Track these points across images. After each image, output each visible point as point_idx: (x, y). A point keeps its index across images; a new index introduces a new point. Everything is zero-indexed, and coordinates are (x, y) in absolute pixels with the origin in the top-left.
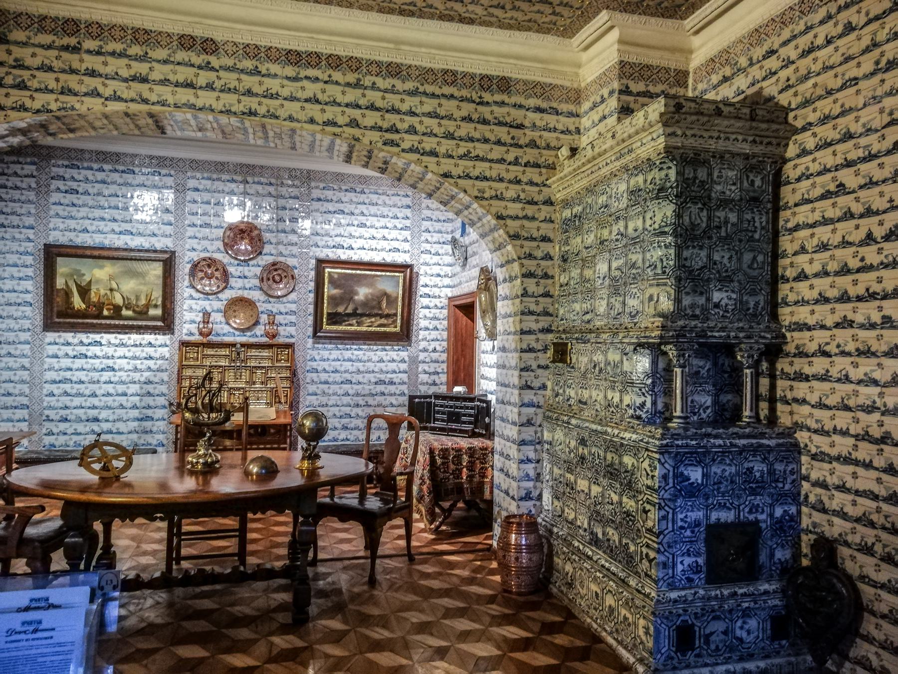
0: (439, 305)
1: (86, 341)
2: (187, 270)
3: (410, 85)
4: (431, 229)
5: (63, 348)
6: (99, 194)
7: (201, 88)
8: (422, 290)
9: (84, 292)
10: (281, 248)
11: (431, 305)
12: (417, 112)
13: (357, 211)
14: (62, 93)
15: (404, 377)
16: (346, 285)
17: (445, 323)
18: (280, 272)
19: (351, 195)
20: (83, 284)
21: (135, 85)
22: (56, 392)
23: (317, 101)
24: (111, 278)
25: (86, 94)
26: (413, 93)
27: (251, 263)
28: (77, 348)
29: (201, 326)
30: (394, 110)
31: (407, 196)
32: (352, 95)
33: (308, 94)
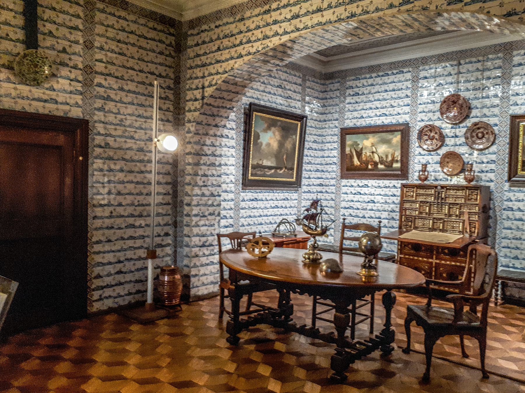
6: (369, 93)
7: (325, 9)
9: (359, 154)
10: (485, 111)
20: (359, 150)
24: (373, 145)
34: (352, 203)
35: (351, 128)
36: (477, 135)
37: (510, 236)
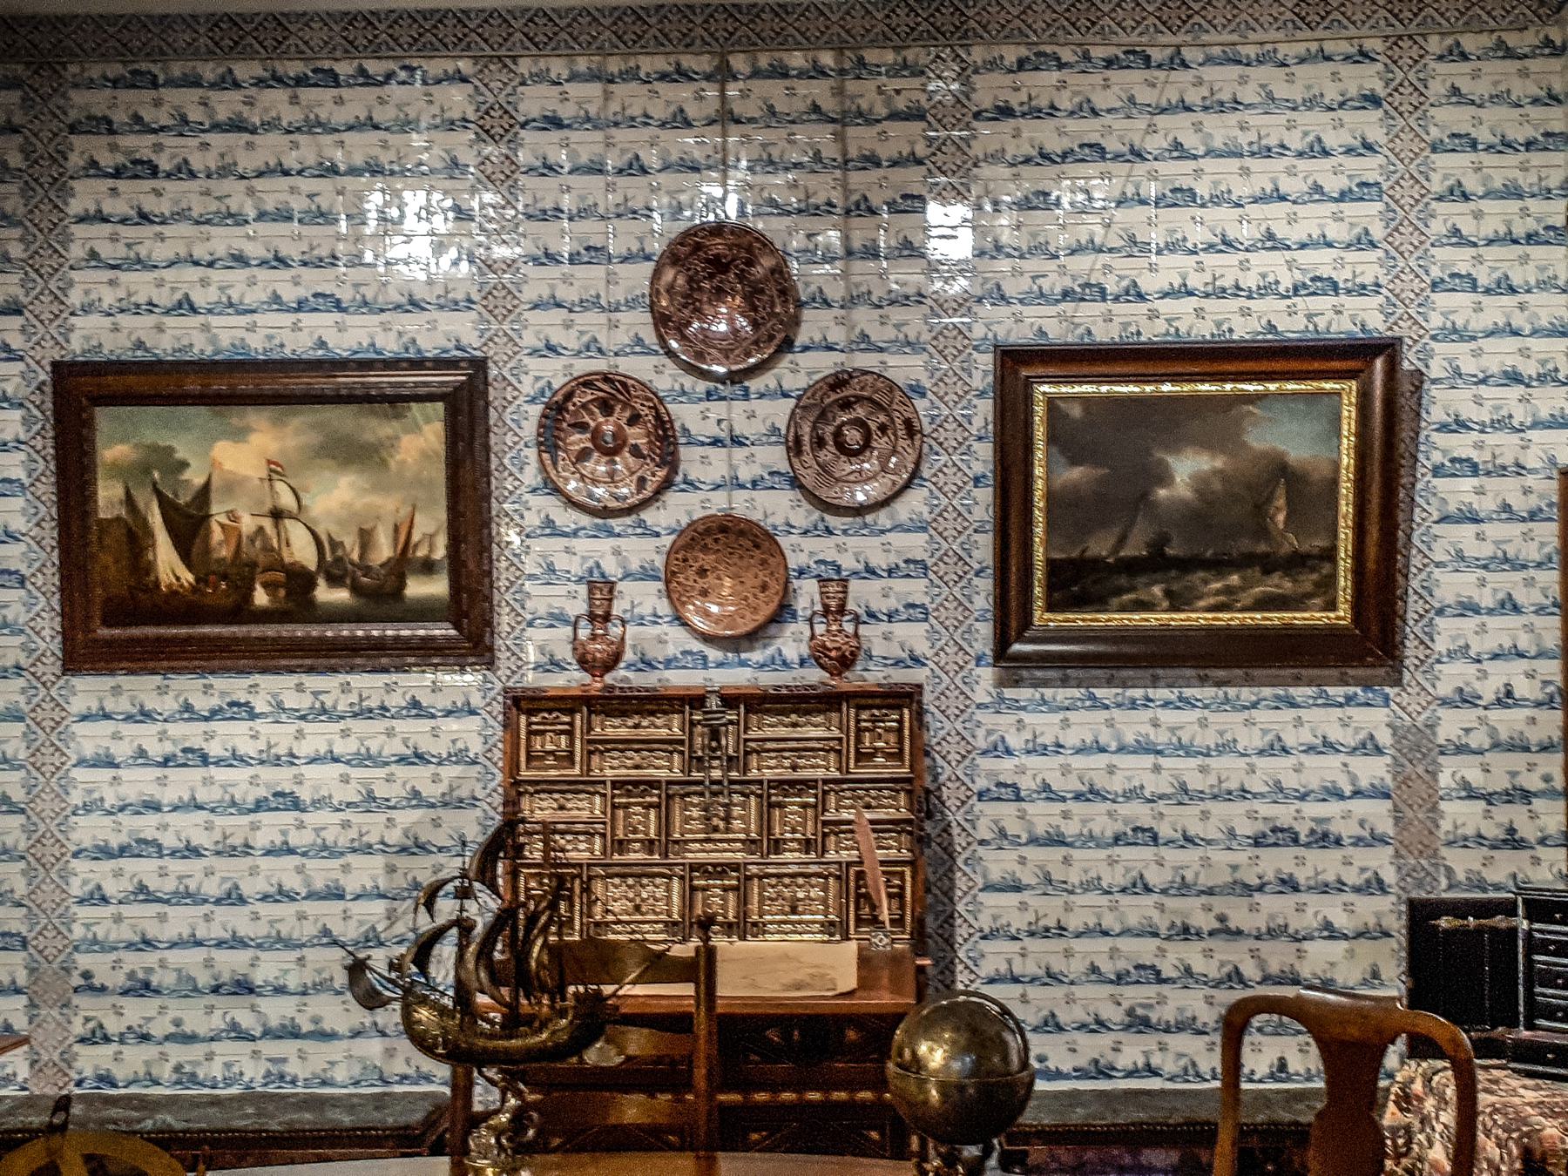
0: (1520, 504)
1: (202, 704)
2: (530, 429)
4: (1472, 184)
5: (128, 729)
6: (225, 171)
8: (1437, 446)
9: (188, 525)
10: (864, 317)
11: (1486, 505)
13: (1154, 144)
15: (1379, 814)
16: (1120, 445)
17: (1550, 579)
18: (860, 412)
19: (1132, 80)
20: (184, 499)
22: (110, 888)
24: (275, 470)
27: (755, 384)
28: (174, 729)
29: (584, 633)
31: (1365, 56)
34: (152, 819)
35: (119, 367)
36: (838, 434)
37: (1019, 922)
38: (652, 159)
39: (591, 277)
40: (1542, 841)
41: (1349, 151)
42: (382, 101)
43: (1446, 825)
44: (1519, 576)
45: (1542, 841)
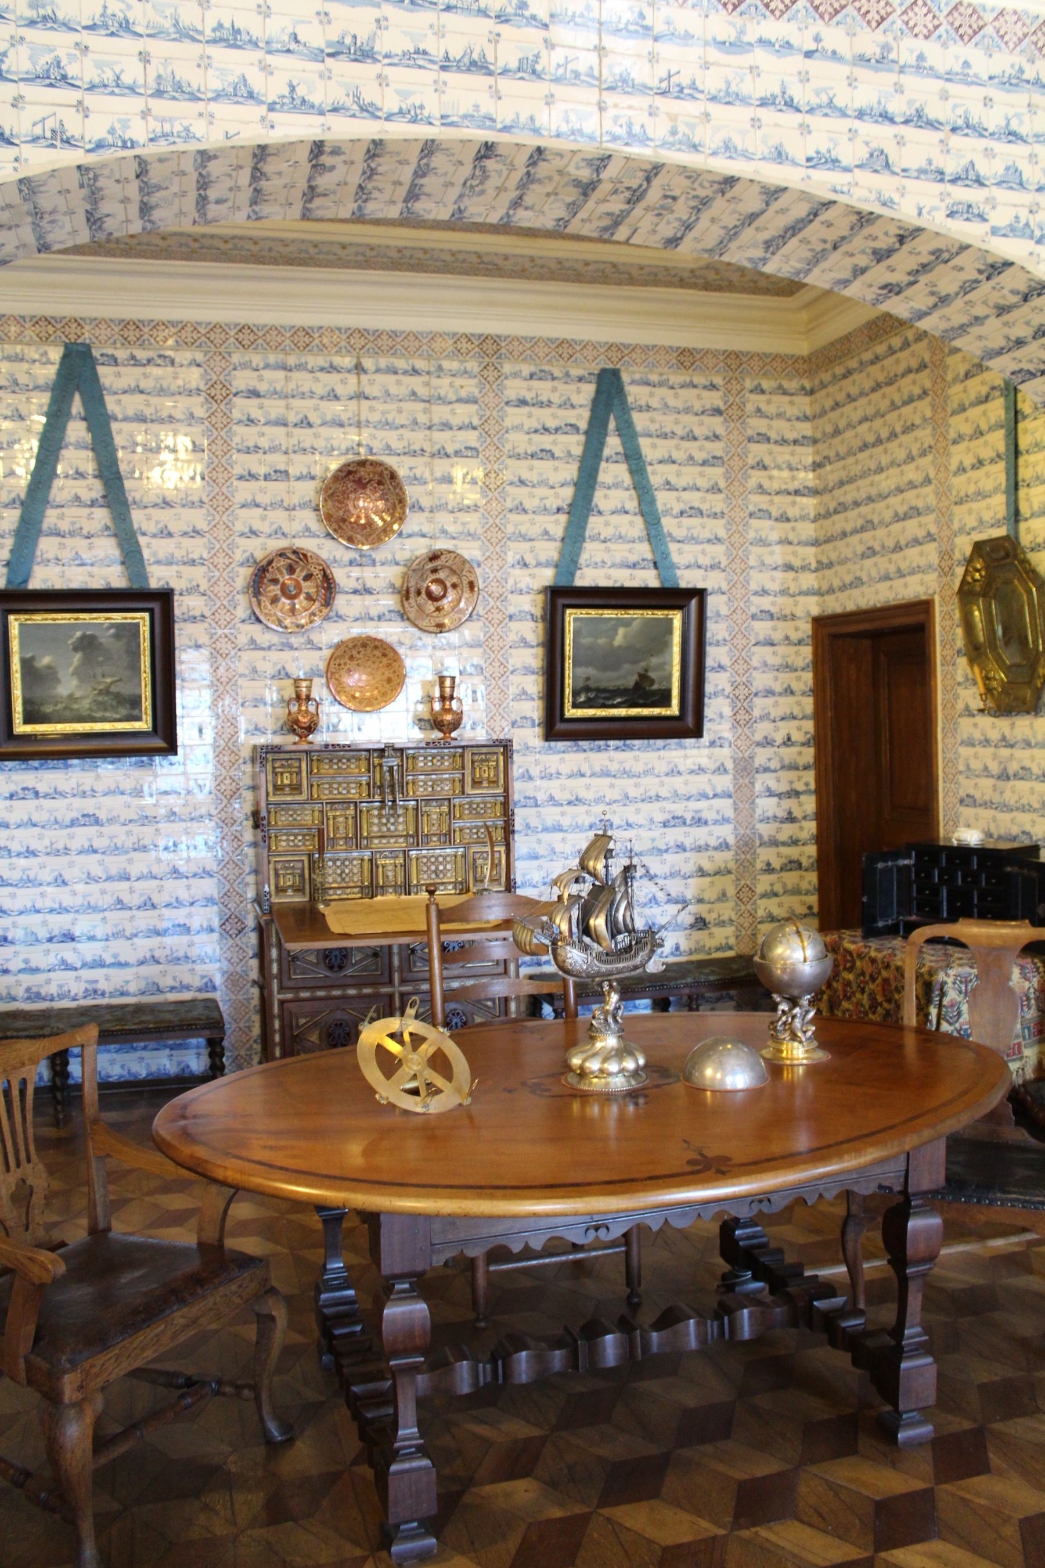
3: (1003, 62)
4: (767, 461)
7: (505, 72)
10: (444, 519)
12: (1023, 131)
14: (159, 94)
17: (808, 677)
18: (441, 575)
21: (339, 66)
23: (790, 104)
25: (219, 96)
26: (1013, 82)
30: (968, 127)
31: (713, 387)
32: (872, 89)
33: (767, 86)
38: (313, 418)
39: (277, 489)
40: (805, 818)
41: (707, 438)
42: (145, 376)
43: (759, 811)
44: (794, 675)
45: (805, 818)
